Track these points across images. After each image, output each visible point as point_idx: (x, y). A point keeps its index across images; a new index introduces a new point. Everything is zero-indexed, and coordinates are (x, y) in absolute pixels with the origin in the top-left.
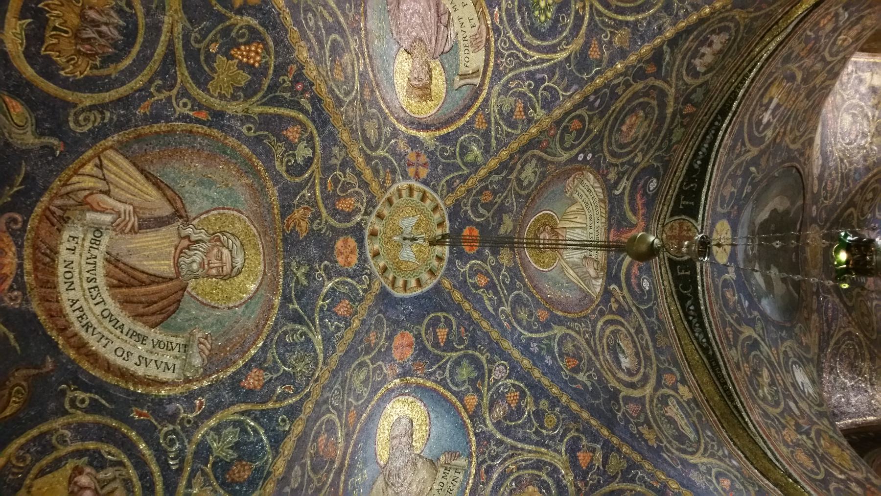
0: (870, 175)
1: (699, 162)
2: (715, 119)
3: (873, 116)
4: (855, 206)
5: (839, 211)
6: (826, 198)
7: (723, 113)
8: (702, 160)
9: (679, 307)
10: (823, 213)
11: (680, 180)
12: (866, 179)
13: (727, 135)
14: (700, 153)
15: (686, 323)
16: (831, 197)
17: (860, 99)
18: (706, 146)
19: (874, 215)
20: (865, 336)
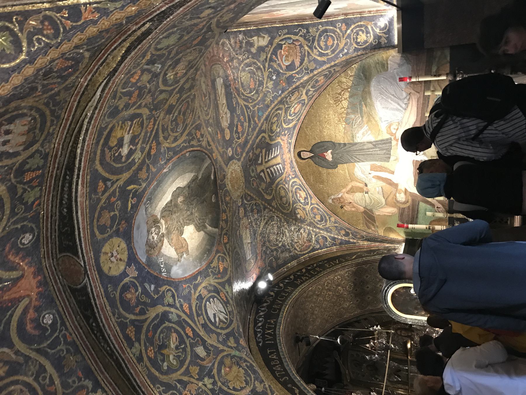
0: (270, 110)
1: (65, 210)
2: (65, 174)
3: (264, 67)
4: (264, 132)
5: (251, 142)
6: (239, 138)
7: (70, 168)
8: (67, 208)
9: (85, 323)
10: (238, 149)
11: (57, 224)
12: (267, 113)
13: (80, 187)
14: (64, 202)
15: (93, 336)
16: (243, 135)
17: (253, 58)
18: (66, 196)
19: (282, 127)
20: (282, 213)
